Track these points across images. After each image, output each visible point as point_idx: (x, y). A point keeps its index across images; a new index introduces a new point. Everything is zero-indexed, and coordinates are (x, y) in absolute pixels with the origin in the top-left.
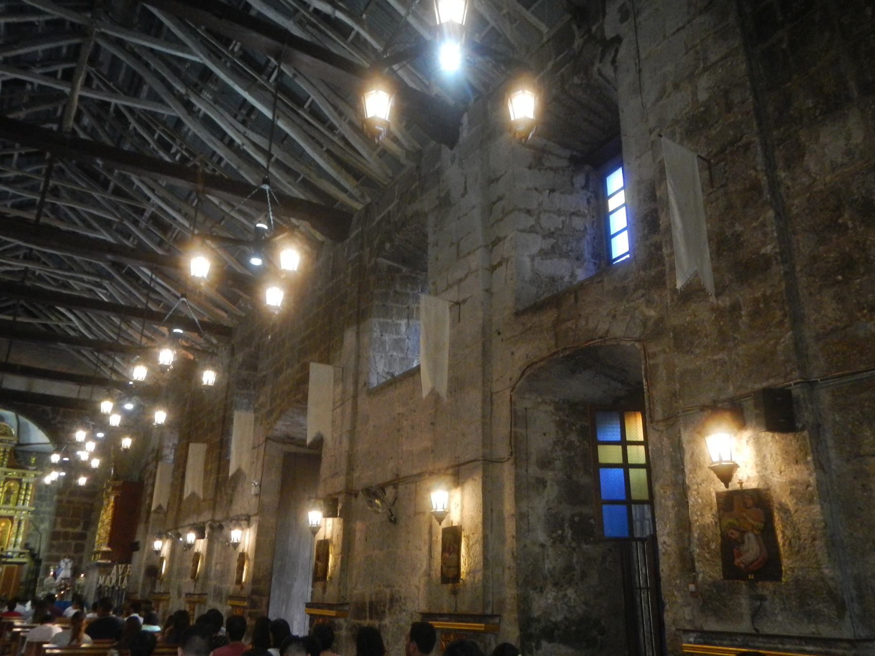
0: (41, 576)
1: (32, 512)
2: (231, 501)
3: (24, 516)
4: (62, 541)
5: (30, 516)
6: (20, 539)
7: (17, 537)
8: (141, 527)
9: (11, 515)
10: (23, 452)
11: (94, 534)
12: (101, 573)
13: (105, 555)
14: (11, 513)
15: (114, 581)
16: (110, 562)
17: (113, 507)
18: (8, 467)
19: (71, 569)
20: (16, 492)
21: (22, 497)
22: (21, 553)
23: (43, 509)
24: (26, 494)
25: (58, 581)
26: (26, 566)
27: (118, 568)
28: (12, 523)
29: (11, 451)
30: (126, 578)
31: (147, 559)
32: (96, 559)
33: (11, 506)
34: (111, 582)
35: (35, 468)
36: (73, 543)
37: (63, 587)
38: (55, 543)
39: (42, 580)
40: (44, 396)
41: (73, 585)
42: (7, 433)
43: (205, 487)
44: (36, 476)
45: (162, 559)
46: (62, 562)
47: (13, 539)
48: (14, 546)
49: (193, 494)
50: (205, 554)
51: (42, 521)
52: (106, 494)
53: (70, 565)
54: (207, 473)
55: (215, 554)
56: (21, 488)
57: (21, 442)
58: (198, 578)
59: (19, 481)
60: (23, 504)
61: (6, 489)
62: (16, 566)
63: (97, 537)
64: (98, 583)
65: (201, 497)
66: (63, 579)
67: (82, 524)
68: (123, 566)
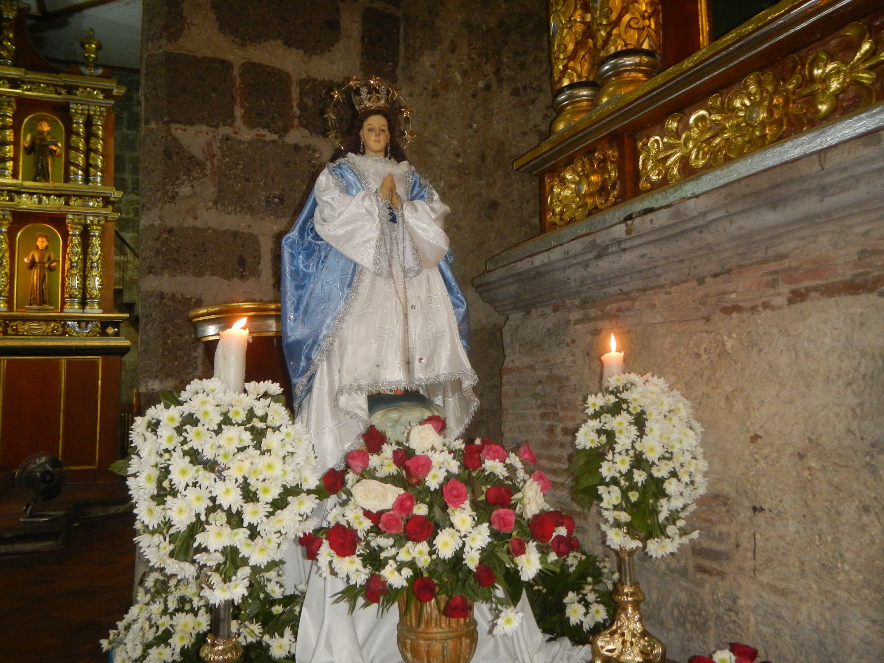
4: (247, 135)
6: (96, 283)
7: (84, 278)
14: (52, 204)
20: (59, 147)
21: (81, 160)
22: (105, 324)
24: (88, 151)
35: (100, 71)
47: (76, 282)
48: (83, 304)
56: (70, 132)
57: (50, 8)
59: (62, 111)
60: (86, 180)
62: (99, 359)
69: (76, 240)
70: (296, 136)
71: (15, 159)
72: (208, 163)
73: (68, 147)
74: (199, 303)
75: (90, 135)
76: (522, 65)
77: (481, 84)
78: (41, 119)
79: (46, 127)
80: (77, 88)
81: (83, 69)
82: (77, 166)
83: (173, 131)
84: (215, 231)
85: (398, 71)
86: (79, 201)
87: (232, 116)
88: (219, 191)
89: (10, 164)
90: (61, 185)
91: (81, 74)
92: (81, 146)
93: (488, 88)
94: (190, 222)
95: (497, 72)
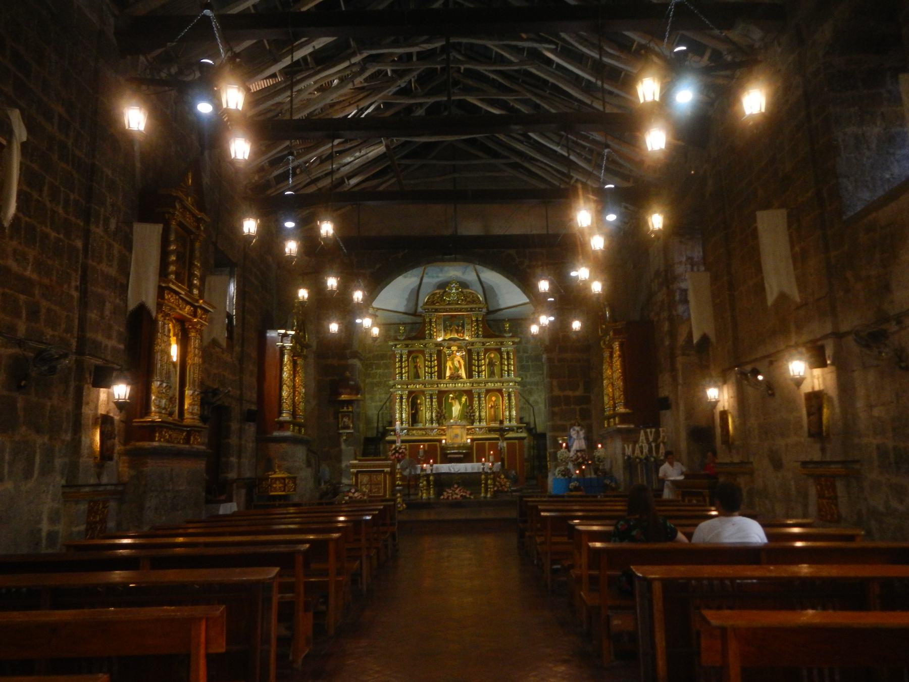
0: (550, 450)
1: (519, 383)
2: (887, 288)
3: (511, 387)
4: (564, 407)
5: (518, 387)
6: (514, 413)
7: (510, 412)
8: (665, 379)
9: (499, 388)
10: (495, 320)
11: (601, 395)
12: (625, 440)
13: (624, 418)
14: (498, 385)
15: (646, 450)
16: (632, 426)
17: (620, 356)
18: (484, 337)
19: (585, 438)
21: (506, 368)
22: (518, 428)
23: (528, 380)
24: (508, 365)
25: (572, 454)
26: (526, 441)
27: (646, 433)
28: (502, 397)
29: (483, 319)
30: (662, 445)
31: (687, 419)
32: (612, 424)
33: (497, 378)
34: (642, 452)
35: (511, 334)
36: (578, 408)
37: (580, 460)
38: (556, 409)
39: (555, 453)
40: (505, 237)
41: (592, 458)
42: (475, 300)
43: (801, 282)
44: (514, 343)
45: (724, 414)
46: (571, 430)
47: (507, 413)
48: (510, 421)
49: (783, 297)
50: (832, 392)
51: (530, 393)
52: (604, 343)
53: (582, 434)
54: (799, 259)
55: (861, 392)
56: (502, 358)
57: (491, 309)
58: (828, 435)
59: (499, 350)
60: (508, 375)
61: (487, 360)
62: (516, 441)
63: (606, 399)
64: (624, 454)
65: (798, 299)
66: (577, 451)
67: (581, 385)
68: (653, 430)
69: (507, 398)
70: (572, 407)
71: (485, 370)
73: (502, 364)
74: (558, 437)
75: (508, 358)
78: (491, 353)
79: (493, 355)
80: (504, 342)
81: (506, 335)
82: (505, 371)
86: (507, 384)
89: (484, 373)
90: (501, 379)
91: (505, 337)
92: (506, 363)
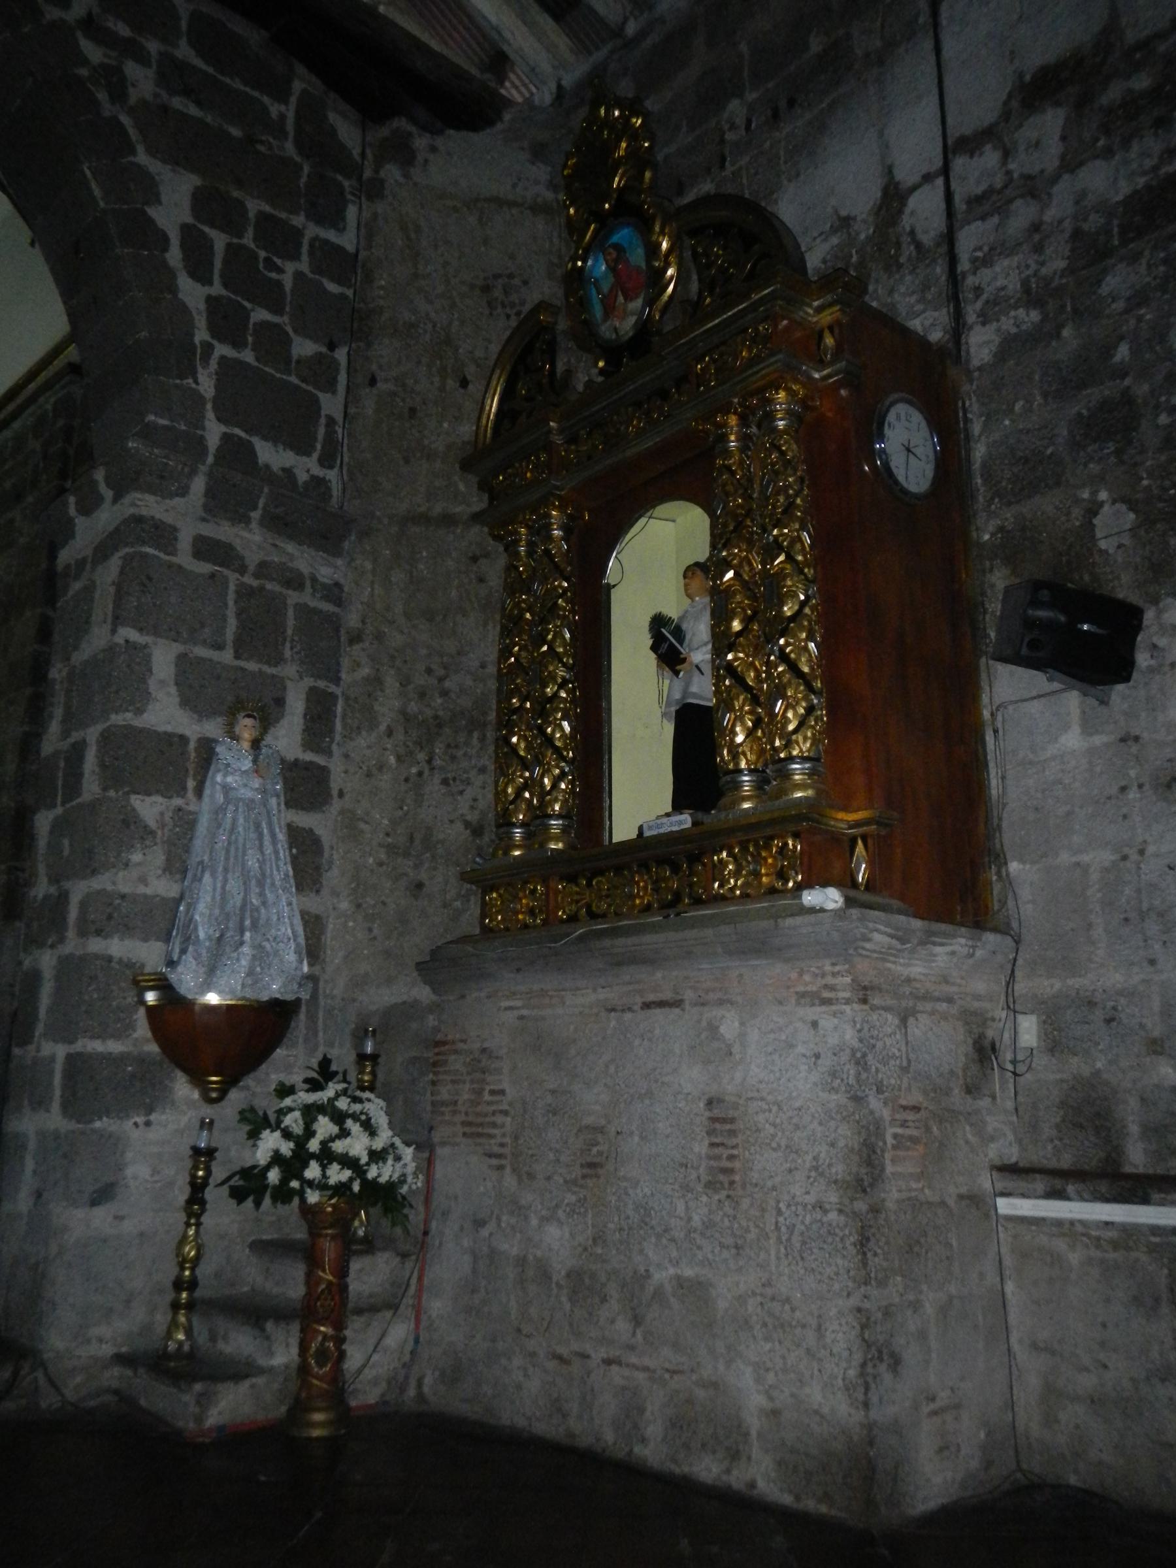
67: (296, 704)
72: (159, 833)
76: (453, 758)
77: (414, 770)
83: (132, 801)
84: (163, 899)
85: (334, 747)
87: (184, 789)
88: (168, 860)
93: (420, 774)
94: (142, 890)
95: (429, 761)
